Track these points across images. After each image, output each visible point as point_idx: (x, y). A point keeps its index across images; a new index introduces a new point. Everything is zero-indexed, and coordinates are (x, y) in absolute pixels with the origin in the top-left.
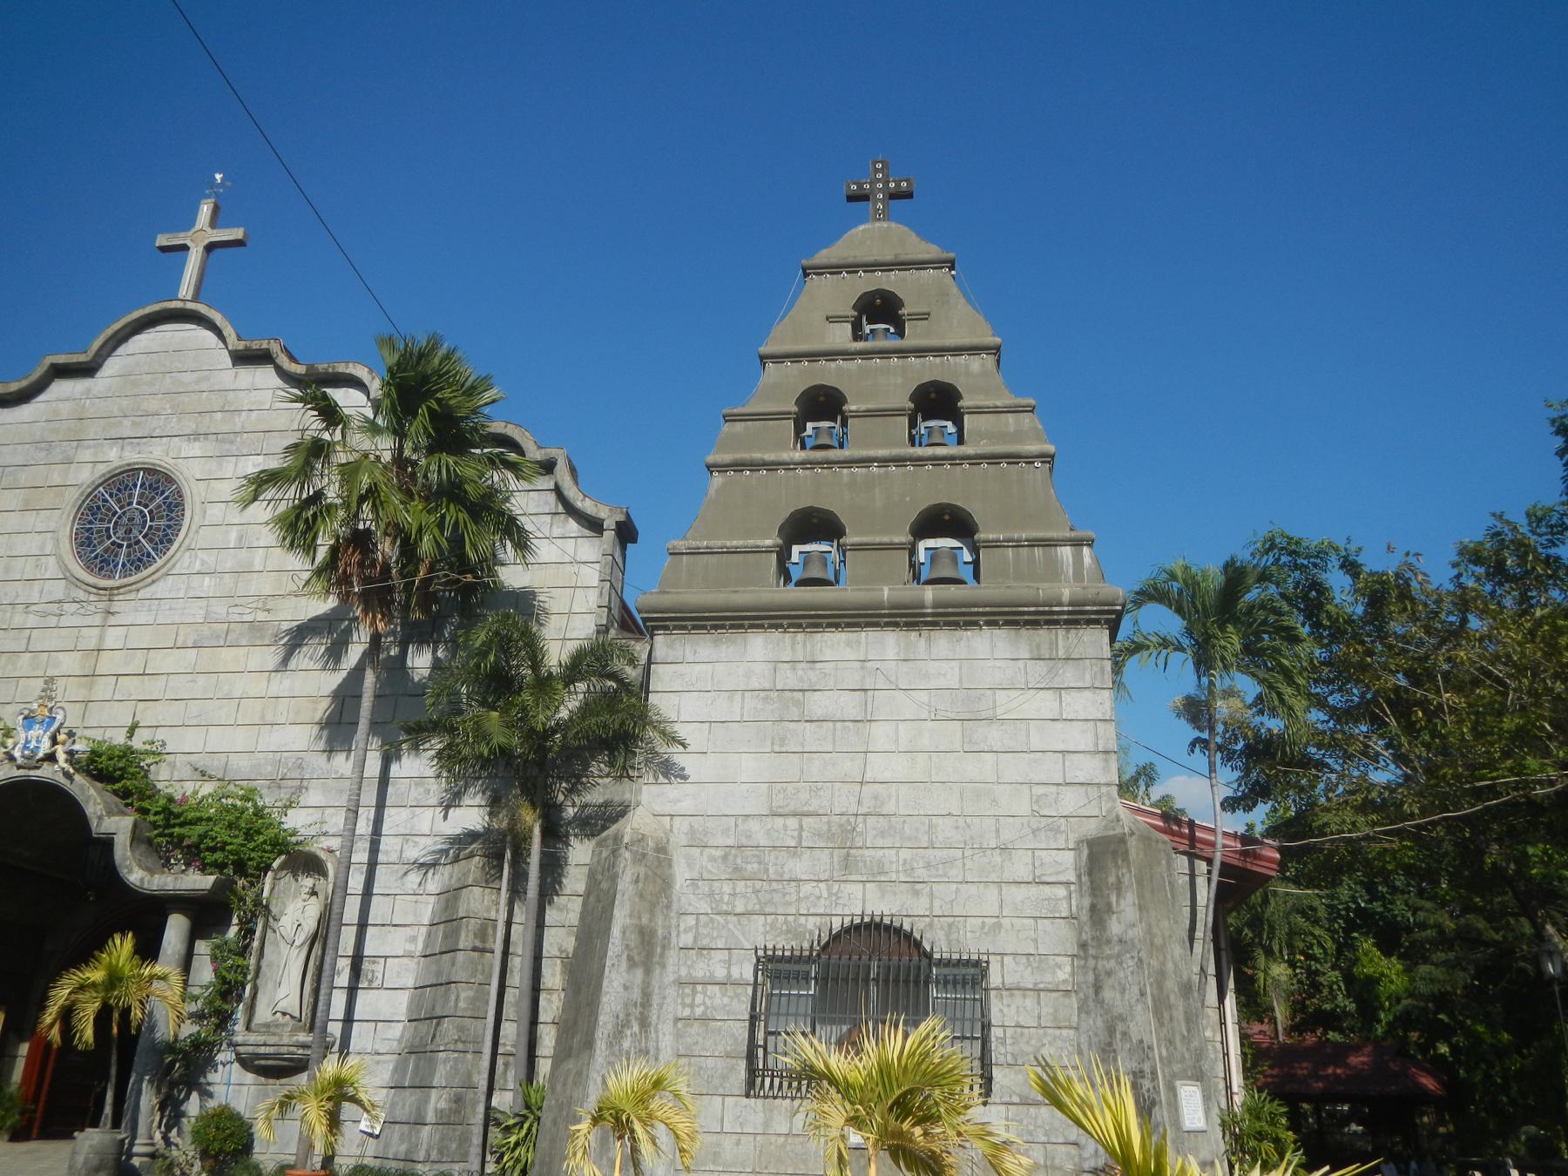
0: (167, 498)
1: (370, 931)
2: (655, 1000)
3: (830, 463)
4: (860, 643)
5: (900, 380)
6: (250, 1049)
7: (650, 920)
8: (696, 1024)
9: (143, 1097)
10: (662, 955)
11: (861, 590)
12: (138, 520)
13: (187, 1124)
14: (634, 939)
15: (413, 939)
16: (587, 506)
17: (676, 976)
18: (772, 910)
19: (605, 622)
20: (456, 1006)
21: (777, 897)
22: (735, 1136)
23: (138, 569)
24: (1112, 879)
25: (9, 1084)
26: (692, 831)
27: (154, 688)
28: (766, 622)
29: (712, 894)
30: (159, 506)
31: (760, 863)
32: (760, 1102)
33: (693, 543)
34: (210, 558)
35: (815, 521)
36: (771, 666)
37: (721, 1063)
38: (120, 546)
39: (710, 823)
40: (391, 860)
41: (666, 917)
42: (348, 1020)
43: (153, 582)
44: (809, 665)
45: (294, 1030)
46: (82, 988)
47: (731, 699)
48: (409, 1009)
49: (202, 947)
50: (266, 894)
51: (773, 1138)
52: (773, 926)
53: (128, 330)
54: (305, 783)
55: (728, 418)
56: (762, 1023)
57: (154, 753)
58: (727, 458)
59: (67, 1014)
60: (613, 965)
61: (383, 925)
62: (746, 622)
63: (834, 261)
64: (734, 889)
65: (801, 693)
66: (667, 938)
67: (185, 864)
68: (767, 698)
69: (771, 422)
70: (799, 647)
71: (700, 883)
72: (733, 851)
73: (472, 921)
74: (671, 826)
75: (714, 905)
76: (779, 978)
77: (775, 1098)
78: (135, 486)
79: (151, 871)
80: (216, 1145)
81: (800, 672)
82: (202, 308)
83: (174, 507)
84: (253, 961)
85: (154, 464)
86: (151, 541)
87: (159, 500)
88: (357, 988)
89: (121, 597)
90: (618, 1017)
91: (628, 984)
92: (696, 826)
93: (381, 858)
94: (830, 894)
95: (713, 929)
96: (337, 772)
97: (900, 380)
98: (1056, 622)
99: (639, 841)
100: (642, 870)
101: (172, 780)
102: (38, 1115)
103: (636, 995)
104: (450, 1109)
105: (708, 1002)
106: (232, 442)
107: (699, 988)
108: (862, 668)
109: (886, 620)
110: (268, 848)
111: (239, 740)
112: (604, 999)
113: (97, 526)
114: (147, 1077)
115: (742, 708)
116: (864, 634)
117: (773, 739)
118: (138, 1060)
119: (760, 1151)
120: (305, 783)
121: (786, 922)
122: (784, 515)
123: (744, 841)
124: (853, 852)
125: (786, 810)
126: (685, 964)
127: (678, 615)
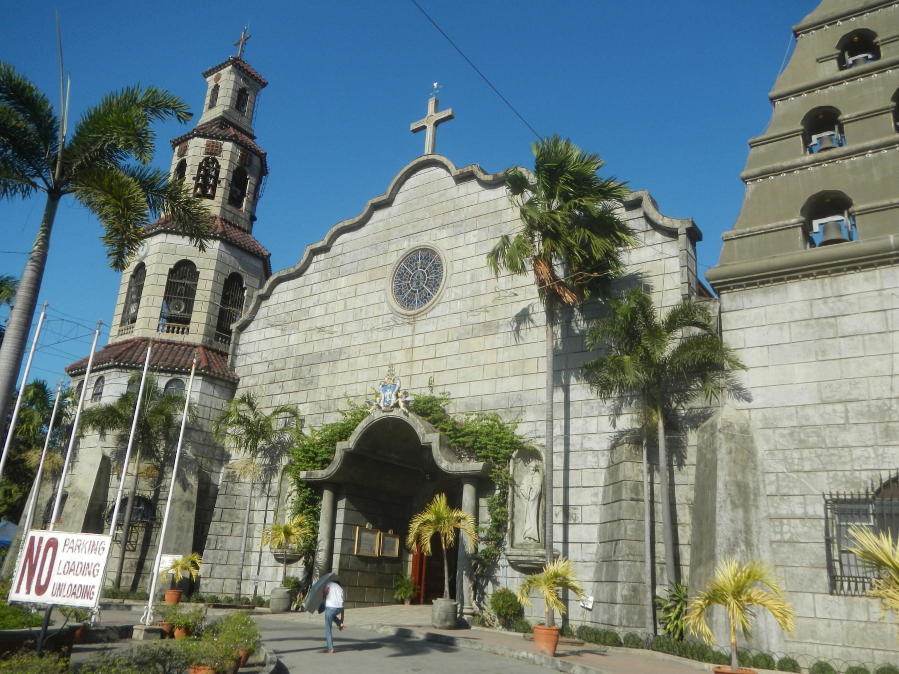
0: (434, 262)
1: (571, 491)
2: (754, 529)
3: (834, 158)
4: (874, 277)
5: (881, 89)
6: (515, 558)
7: (744, 477)
8: (786, 545)
9: (464, 583)
10: (755, 500)
11: (870, 240)
12: (422, 277)
13: (488, 599)
14: (733, 490)
15: (596, 495)
16: (666, 222)
17: (767, 514)
18: (833, 468)
19: (687, 292)
20: (626, 533)
21: (834, 459)
22: (826, 621)
23: (425, 302)
25: (406, 575)
26: (765, 418)
27: (441, 364)
28: (800, 274)
29: (785, 459)
30: (431, 268)
31: (818, 436)
32: (841, 598)
33: (740, 231)
34: (458, 291)
35: (828, 200)
36: (807, 303)
37: (808, 572)
38: (415, 292)
39: (777, 412)
40: (577, 449)
41: (754, 475)
42: (566, 542)
43: (433, 308)
44: (837, 298)
45: (536, 548)
46: (424, 524)
47: (781, 329)
48: (599, 536)
49: (483, 502)
50: (511, 472)
51: (856, 624)
52: (834, 478)
53: (403, 178)
54: (524, 408)
55: (753, 145)
56: (836, 545)
57: (445, 399)
58: (756, 170)
59: (418, 538)
60: (721, 507)
61: (577, 487)
62: (785, 276)
63: (816, 20)
64: (801, 455)
65: (833, 319)
66: (757, 489)
67: (469, 457)
68: (808, 325)
69: (784, 141)
70: (828, 288)
71: (776, 452)
72: (797, 430)
73: (628, 482)
74: (750, 416)
75: (788, 466)
76: (844, 514)
77: (853, 596)
78: (418, 259)
79: (451, 462)
80: (504, 610)
81: (831, 305)
82: (436, 157)
83: (437, 267)
84: (509, 509)
86: (429, 286)
87: (430, 264)
88: (568, 524)
89: (419, 319)
90: (729, 539)
91: (733, 519)
92: (768, 415)
93: (571, 448)
94: (877, 455)
95: (789, 482)
96: (540, 401)
97: (881, 89)
99: (728, 427)
100: (733, 445)
101: (456, 412)
102: (422, 592)
103: (740, 525)
104: (630, 595)
105: (793, 530)
106: (461, 226)
107: (785, 521)
108: (880, 295)
109: (895, 258)
110: (509, 446)
111: (485, 388)
112: (718, 528)
113: (403, 283)
114: (464, 572)
115: (790, 334)
116: (877, 272)
117: (816, 352)
118: (460, 563)
119: (847, 632)
120: (524, 408)
121: (844, 476)
122: (804, 200)
123: (804, 423)
124: (891, 424)
125: (834, 399)
126: (772, 506)
127: (735, 278)
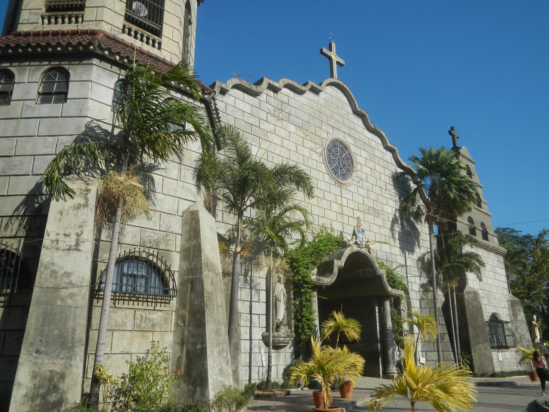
24: (517, 309)
98: (499, 254)
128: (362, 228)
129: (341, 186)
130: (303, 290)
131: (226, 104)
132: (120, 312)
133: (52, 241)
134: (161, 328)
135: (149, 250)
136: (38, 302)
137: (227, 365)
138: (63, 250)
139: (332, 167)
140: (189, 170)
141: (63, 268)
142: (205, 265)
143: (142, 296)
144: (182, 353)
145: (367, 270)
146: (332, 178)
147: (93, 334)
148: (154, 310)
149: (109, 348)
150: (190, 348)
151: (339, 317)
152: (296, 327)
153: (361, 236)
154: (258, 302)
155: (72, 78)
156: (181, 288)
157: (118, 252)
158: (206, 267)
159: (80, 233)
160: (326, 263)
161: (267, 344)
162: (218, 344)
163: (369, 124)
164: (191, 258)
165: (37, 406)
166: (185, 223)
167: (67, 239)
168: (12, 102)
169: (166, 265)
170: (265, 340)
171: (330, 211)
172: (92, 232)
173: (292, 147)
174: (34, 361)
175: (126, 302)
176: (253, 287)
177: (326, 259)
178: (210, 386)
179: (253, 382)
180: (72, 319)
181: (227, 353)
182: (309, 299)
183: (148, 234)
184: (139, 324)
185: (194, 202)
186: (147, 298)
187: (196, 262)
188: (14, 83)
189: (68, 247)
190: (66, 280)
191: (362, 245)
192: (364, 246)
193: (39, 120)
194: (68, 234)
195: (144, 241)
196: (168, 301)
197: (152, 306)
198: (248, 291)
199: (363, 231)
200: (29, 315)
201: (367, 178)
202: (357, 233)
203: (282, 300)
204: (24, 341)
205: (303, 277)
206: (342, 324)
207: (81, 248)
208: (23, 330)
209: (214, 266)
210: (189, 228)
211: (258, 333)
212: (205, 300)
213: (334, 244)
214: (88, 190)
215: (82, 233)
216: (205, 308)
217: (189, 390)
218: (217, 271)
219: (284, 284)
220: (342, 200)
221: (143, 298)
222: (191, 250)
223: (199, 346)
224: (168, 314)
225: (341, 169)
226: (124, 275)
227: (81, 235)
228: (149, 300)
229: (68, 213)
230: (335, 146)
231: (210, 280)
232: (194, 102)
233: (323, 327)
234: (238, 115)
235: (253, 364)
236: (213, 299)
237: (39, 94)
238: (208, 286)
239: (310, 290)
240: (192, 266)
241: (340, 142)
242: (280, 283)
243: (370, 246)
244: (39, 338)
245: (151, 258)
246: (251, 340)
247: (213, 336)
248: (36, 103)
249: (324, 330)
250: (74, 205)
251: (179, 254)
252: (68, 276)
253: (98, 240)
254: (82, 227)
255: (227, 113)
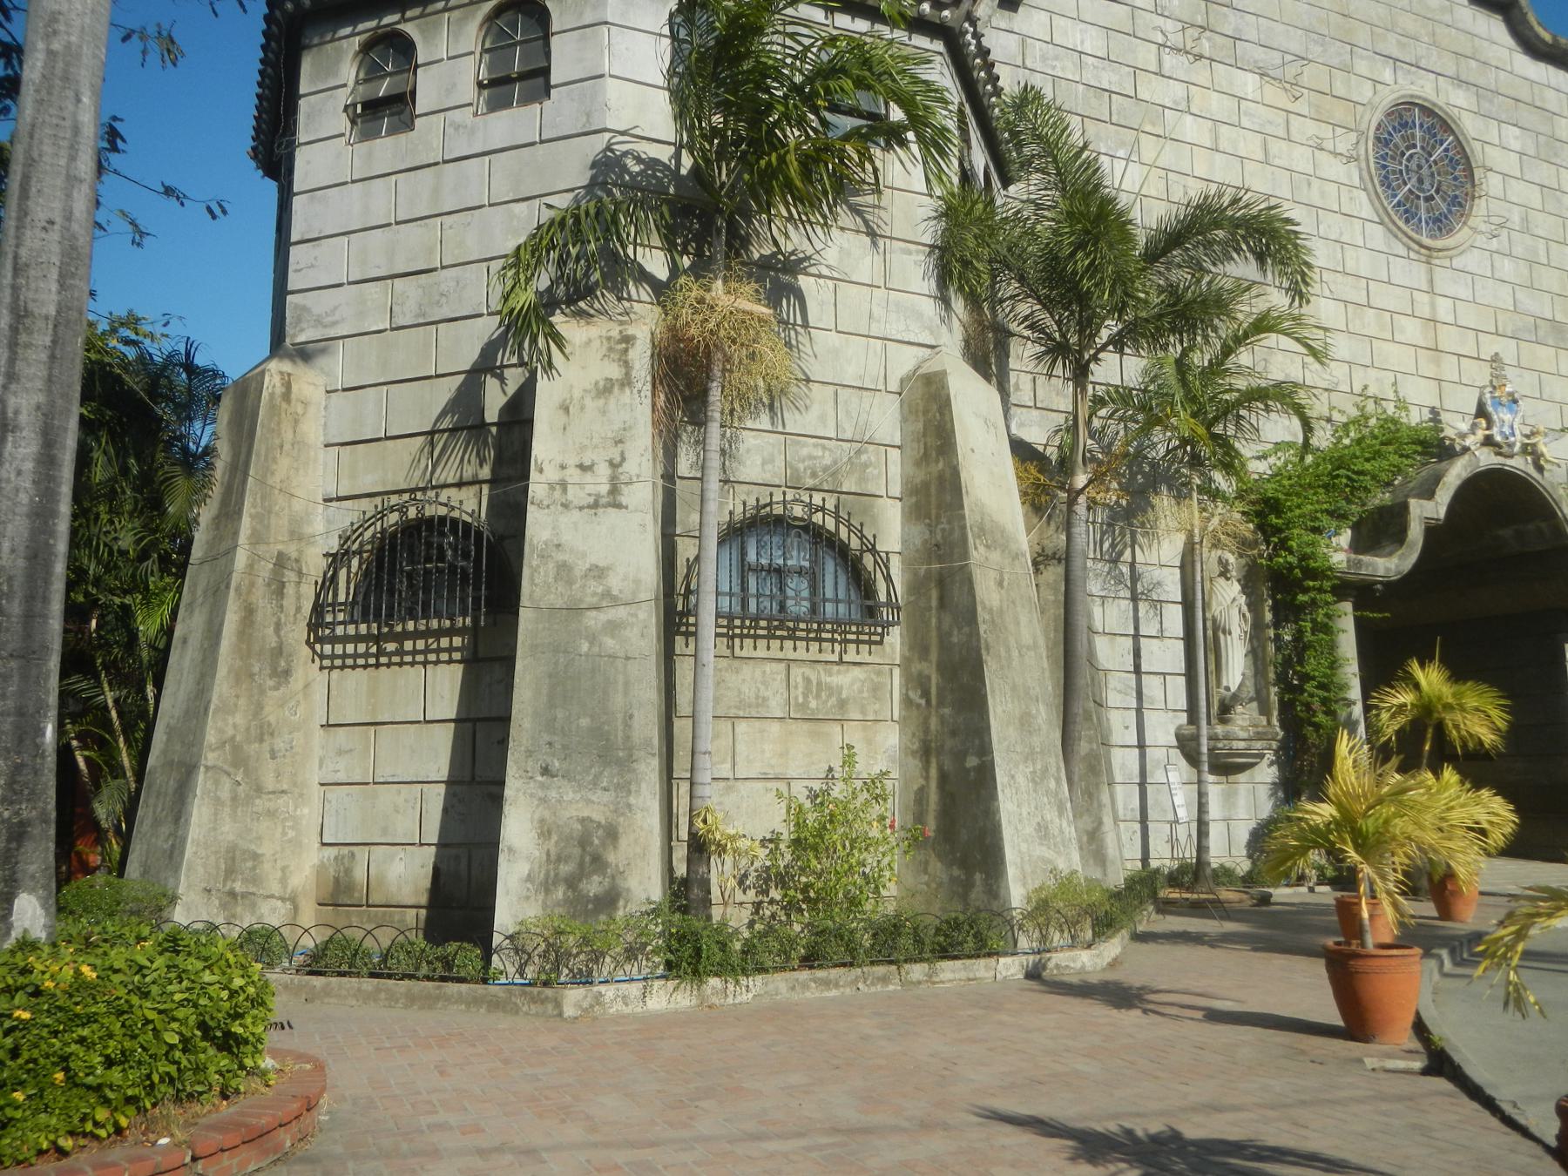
85: (1434, 104)
106: (1491, 102)
128: (1508, 389)
129: (1430, 257)
130: (1302, 598)
131: (1024, 37)
132: (747, 670)
133: (552, 486)
134: (863, 712)
135: (811, 497)
136: (534, 647)
137: (1061, 815)
138: (581, 508)
139: (1395, 196)
140: (910, 253)
141: (584, 555)
142: (975, 529)
143: (802, 626)
144: (927, 778)
145: (1531, 527)
146: (1394, 232)
147: (682, 727)
148: (841, 662)
149: (728, 766)
150: (948, 765)
151: (1431, 678)
152: (1286, 708)
153: (1507, 417)
154: (1160, 636)
155: (555, 27)
156: (912, 598)
157: (723, 507)
158: (979, 537)
159: (619, 459)
160: (1382, 511)
161: (1192, 758)
162: (1030, 756)
163: (1532, 28)
164: (934, 512)
165: (558, 904)
166: (910, 412)
167: (588, 477)
168: (418, 122)
169: (862, 537)
170: (1187, 746)
171: (1391, 344)
172: (649, 455)
173: (1250, 146)
174: (541, 794)
175: (762, 643)
176: (1142, 593)
177: (1381, 498)
178: (1012, 872)
179: (1154, 864)
180: (620, 687)
181: (1058, 780)
182: (1326, 625)
183: (805, 452)
184: (801, 700)
185: (932, 347)
186: (819, 630)
187: (949, 522)
188: (417, 66)
189: (591, 500)
190: (595, 587)
191: (1511, 445)
192: (1517, 448)
193: (487, 158)
194: (588, 463)
195: (797, 470)
196: (878, 638)
197: (833, 651)
198: (1126, 605)
199: (1515, 401)
200: (517, 680)
201: (1525, 220)
202: (1490, 409)
203: (1236, 631)
204: (511, 744)
205: (1304, 557)
206: (1440, 698)
207: (624, 500)
208: (505, 720)
209: (1003, 532)
210: (920, 426)
211: (1163, 728)
212: (982, 632)
213: (1409, 449)
214: (628, 340)
215: (623, 459)
216: (984, 652)
217: (953, 880)
218: (1013, 547)
219: (1239, 581)
220: (1433, 306)
221: (808, 631)
222: (933, 491)
223: (972, 762)
224: (879, 673)
225: (1429, 199)
226: (750, 569)
227: (620, 465)
228: (824, 635)
229: (582, 408)
230: (1404, 125)
231: (993, 575)
232: (910, 39)
233: (1377, 707)
234: (1063, 69)
235: (1152, 814)
236: (1006, 629)
237: (480, 85)
238: (987, 592)
239: (1329, 598)
240: (939, 537)
241: (1422, 108)
242: (1228, 579)
243: (1542, 448)
244: (546, 737)
245: (818, 518)
246: (1141, 746)
247: (1012, 733)
248: (476, 114)
249: (1378, 715)
250: (596, 383)
251: (899, 504)
252: (600, 577)
253: (669, 476)
254: (621, 441)
255: (1029, 64)
